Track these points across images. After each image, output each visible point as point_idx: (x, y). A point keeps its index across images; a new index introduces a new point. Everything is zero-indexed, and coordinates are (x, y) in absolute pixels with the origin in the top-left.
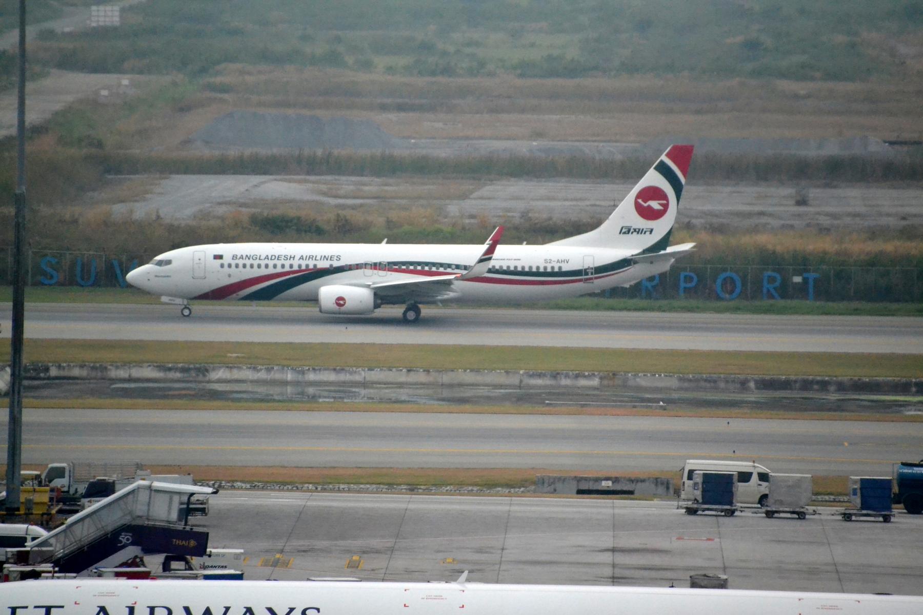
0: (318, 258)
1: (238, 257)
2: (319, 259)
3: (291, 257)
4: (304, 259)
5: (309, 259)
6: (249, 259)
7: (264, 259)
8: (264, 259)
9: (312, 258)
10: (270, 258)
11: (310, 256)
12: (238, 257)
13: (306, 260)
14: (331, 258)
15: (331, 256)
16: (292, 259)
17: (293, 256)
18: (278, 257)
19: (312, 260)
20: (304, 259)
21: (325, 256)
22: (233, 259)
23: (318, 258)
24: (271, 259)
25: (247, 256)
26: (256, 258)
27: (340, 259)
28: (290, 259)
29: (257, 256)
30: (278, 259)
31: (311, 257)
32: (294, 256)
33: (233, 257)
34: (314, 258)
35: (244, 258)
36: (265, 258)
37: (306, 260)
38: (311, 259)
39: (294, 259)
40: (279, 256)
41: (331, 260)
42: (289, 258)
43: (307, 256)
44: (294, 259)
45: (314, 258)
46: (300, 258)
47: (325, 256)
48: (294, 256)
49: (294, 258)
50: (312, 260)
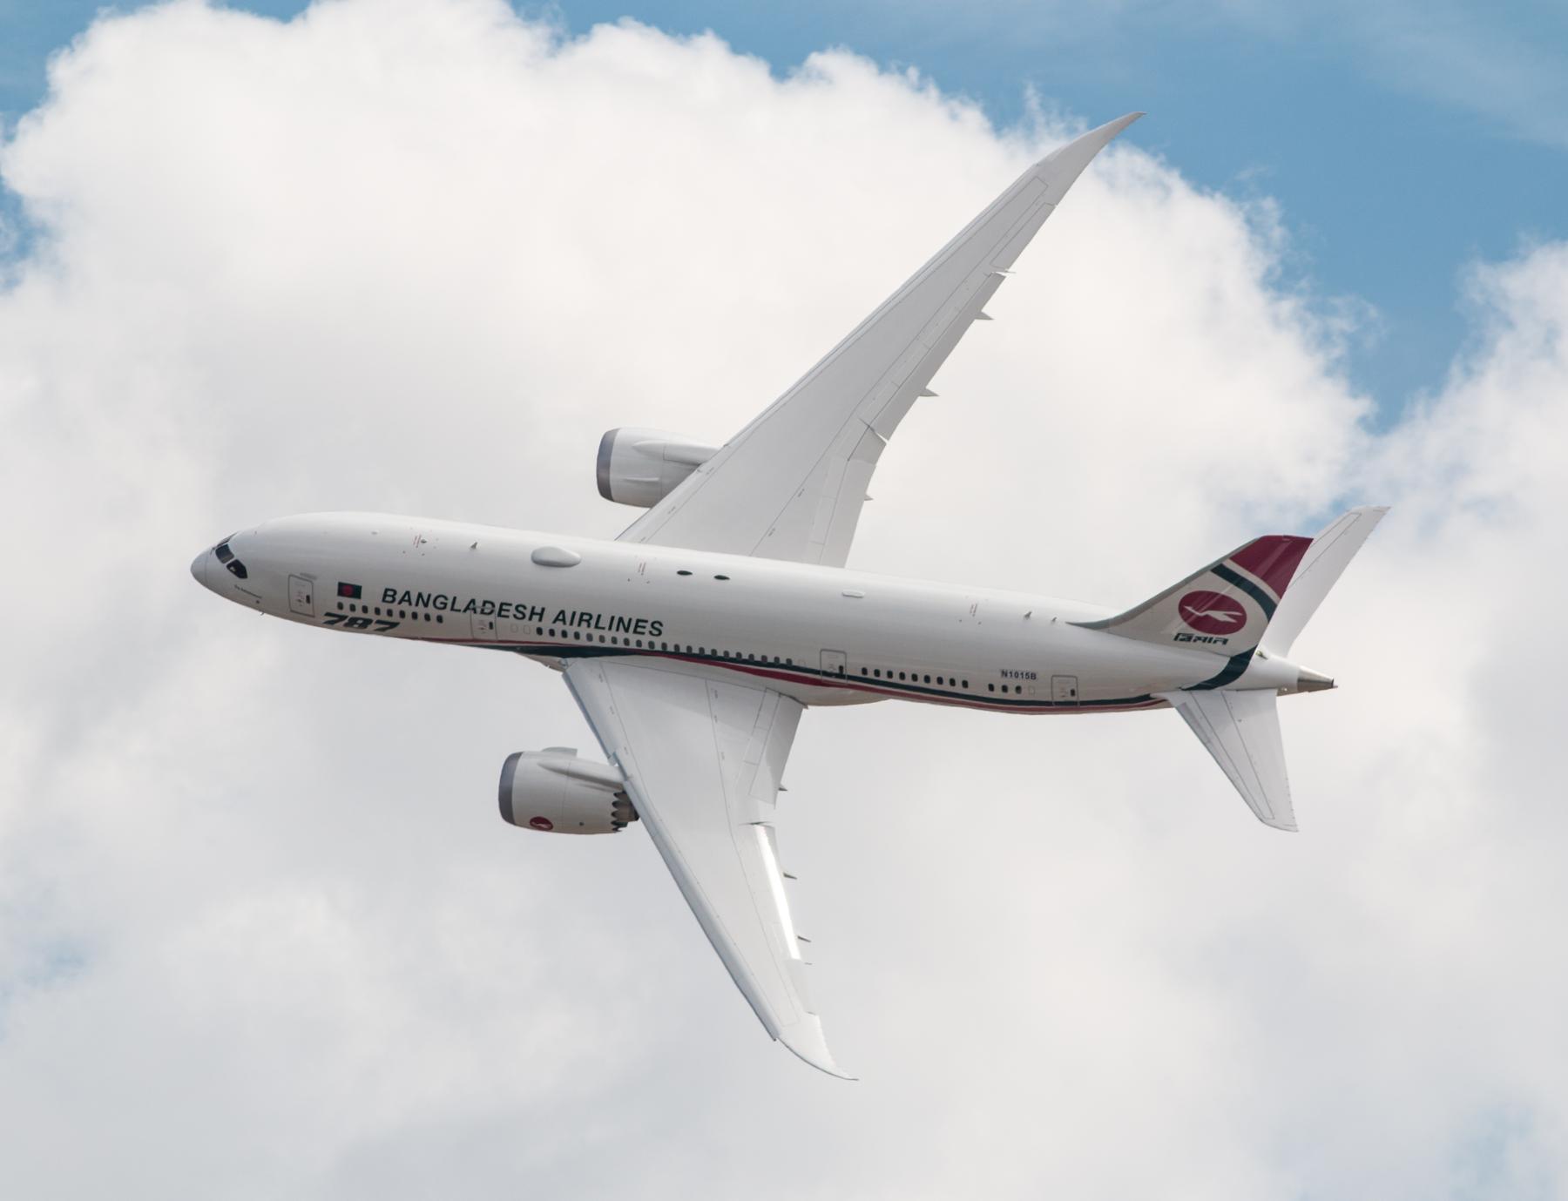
0: (604, 622)
1: (398, 597)
2: (607, 628)
3: (533, 613)
4: (568, 620)
5: (579, 625)
6: (426, 605)
7: (465, 611)
8: (465, 611)
9: (588, 621)
10: (479, 610)
11: (582, 614)
12: (398, 597)
13: (571, 624)
14: (637, 626)
15: (638, 621)
16: (536, 618)
17: (538, 610)
18: (501, 609)
19: (589, 626)
20: (568, 620)
21: (621, 620)
22: (384, 600)
23: (604, 622)
24: (482, 612)
25: (420, 595)
26: (446, 604)
27: (660, 633)
28: (530, 619)
29: (446, 598)
30: (499, 615)
31: (586, 617)
32: (543, 610)
33: (385, 595)
34: (593, 622)
35: (414, 602)
36: (467, 608)
37: (571, 624)
38: (584, 624)
39: (540, 620)
40: (502, 604)
41: (635, 632)
42: (528, 613)
43: (574, 614)
44: (540, 620)
45: (593, 622)
46: (557, 619)
47: (621, 620)
48: (543, 610)
49: (541, 615)
50: (589, 626)
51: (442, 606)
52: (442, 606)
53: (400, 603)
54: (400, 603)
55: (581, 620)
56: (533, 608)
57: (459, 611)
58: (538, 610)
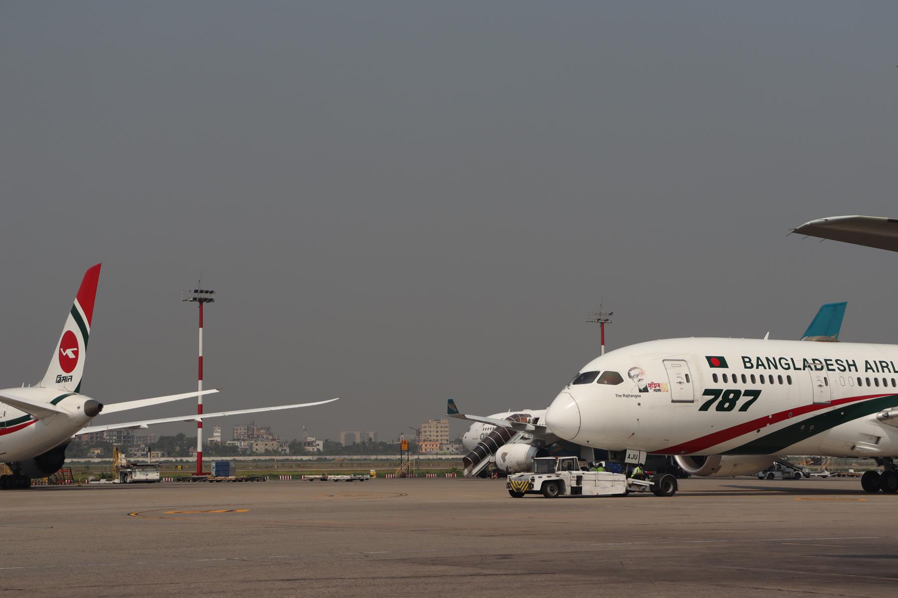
3: (849, 365)
6: (776, 367)
13: (878, 371)
22: (746, 367)
26: (788, 364)
32: (853, 361)
48: (853, 361)
49: (854, 365)
51: (787, 366)
52: (787, 366)
53: (757, 368)
54: (757, 368)
55: (883, 367)
56: (847, 361)
57: (800, 369)
58: (851, 363)
